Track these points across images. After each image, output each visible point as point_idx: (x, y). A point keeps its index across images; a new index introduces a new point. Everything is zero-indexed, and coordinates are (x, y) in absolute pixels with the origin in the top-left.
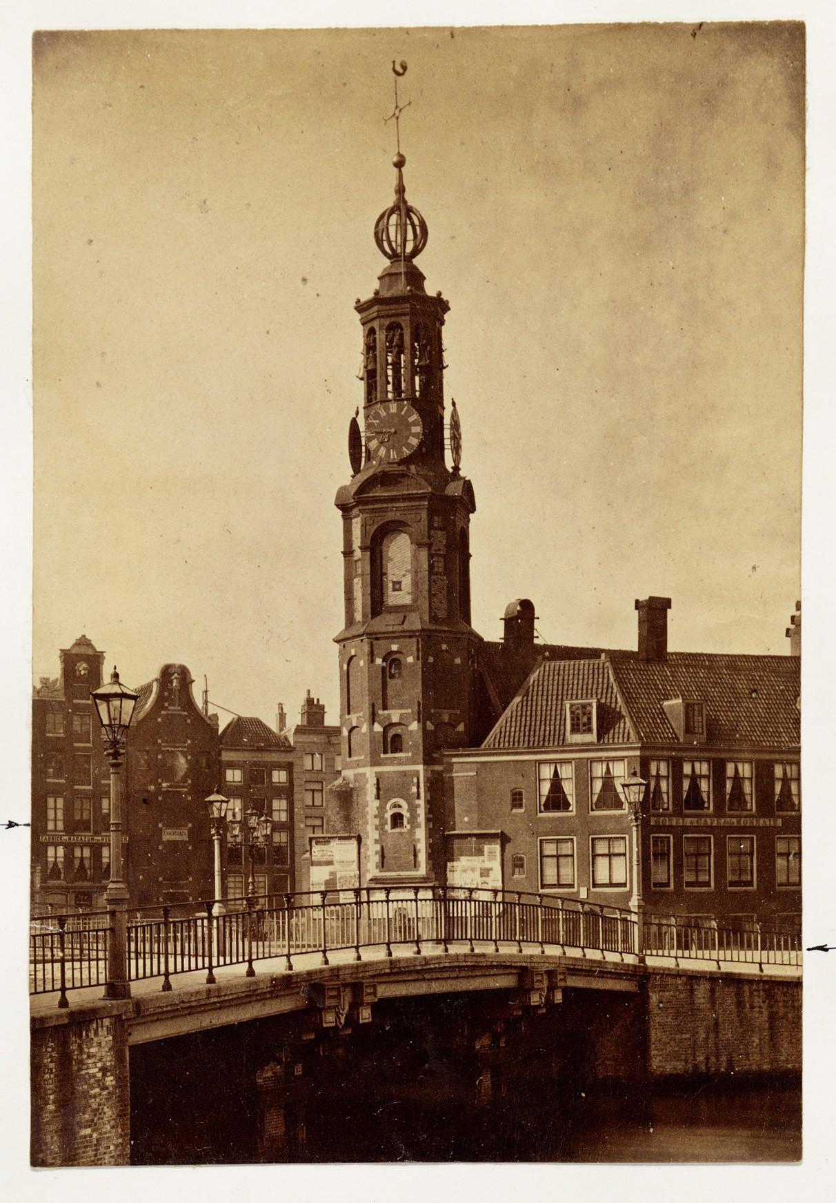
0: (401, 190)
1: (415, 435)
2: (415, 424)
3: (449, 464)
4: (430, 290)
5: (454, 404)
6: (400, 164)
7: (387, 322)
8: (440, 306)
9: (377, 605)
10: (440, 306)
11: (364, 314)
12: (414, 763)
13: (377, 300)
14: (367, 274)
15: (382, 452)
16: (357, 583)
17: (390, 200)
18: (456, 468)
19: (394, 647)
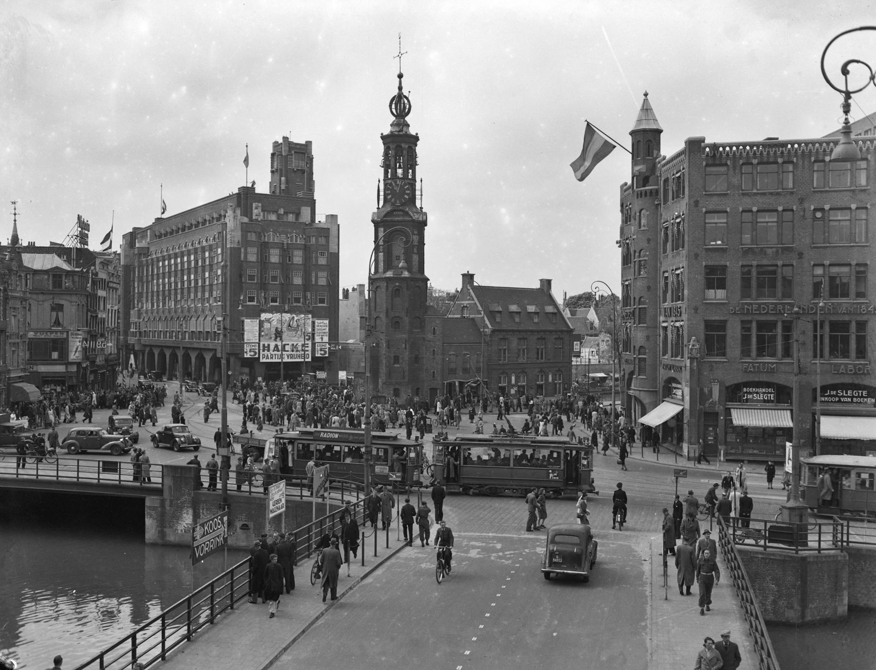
0: (400, 88)
1: (408, 194)
4: (412, 131)
6: (400, 76)
8: (416, 138)
10: (416, 138)
18: (421, 208)
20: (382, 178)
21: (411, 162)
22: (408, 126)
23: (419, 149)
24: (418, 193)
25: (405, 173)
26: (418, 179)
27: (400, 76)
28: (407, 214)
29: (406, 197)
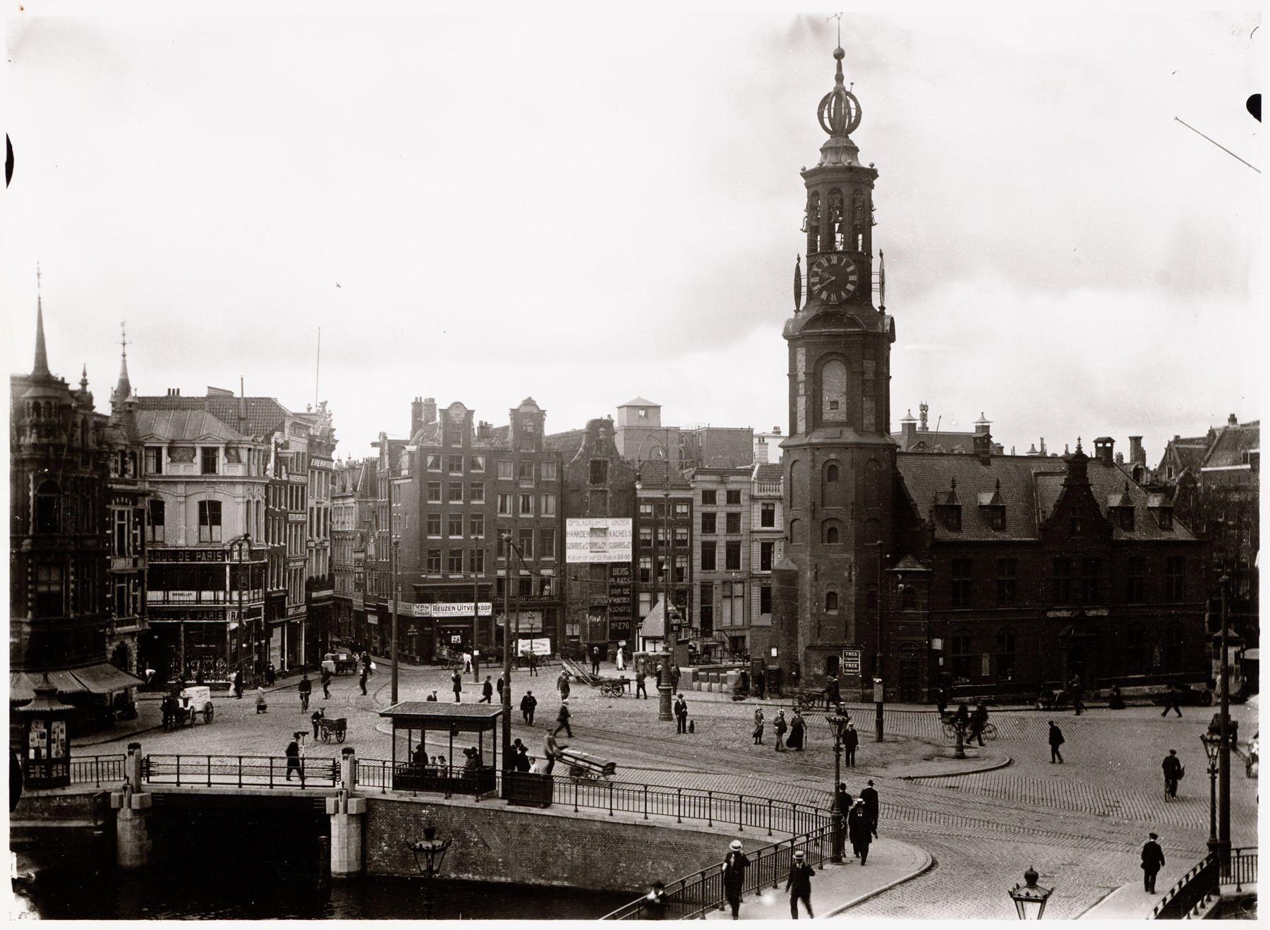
0: (839, 78)
1: (852, 283)
2: (852, 273)
3: (876, 304)
4: (864, 161)
5: (881, 255)
6: (839, 55)
7: (831, 186)
8: (872, 174)
9: (815, 419)
11: (813, 179)
12: (846, 551)
13: (820, 170)
14: (811, 146)
15: (824, 295)
16: (802, 402)
17: (831, 86)
18: (882, 308)
19: (833, 456)
20: (803, 251)
21: (861, 219)
22: (857, 150)
23: (879, 195)
24: (875, 279)
25: (851, 243)
26: (875, 253)
27: (839, 55)
28: (853, 322)
29: (850, 287)
